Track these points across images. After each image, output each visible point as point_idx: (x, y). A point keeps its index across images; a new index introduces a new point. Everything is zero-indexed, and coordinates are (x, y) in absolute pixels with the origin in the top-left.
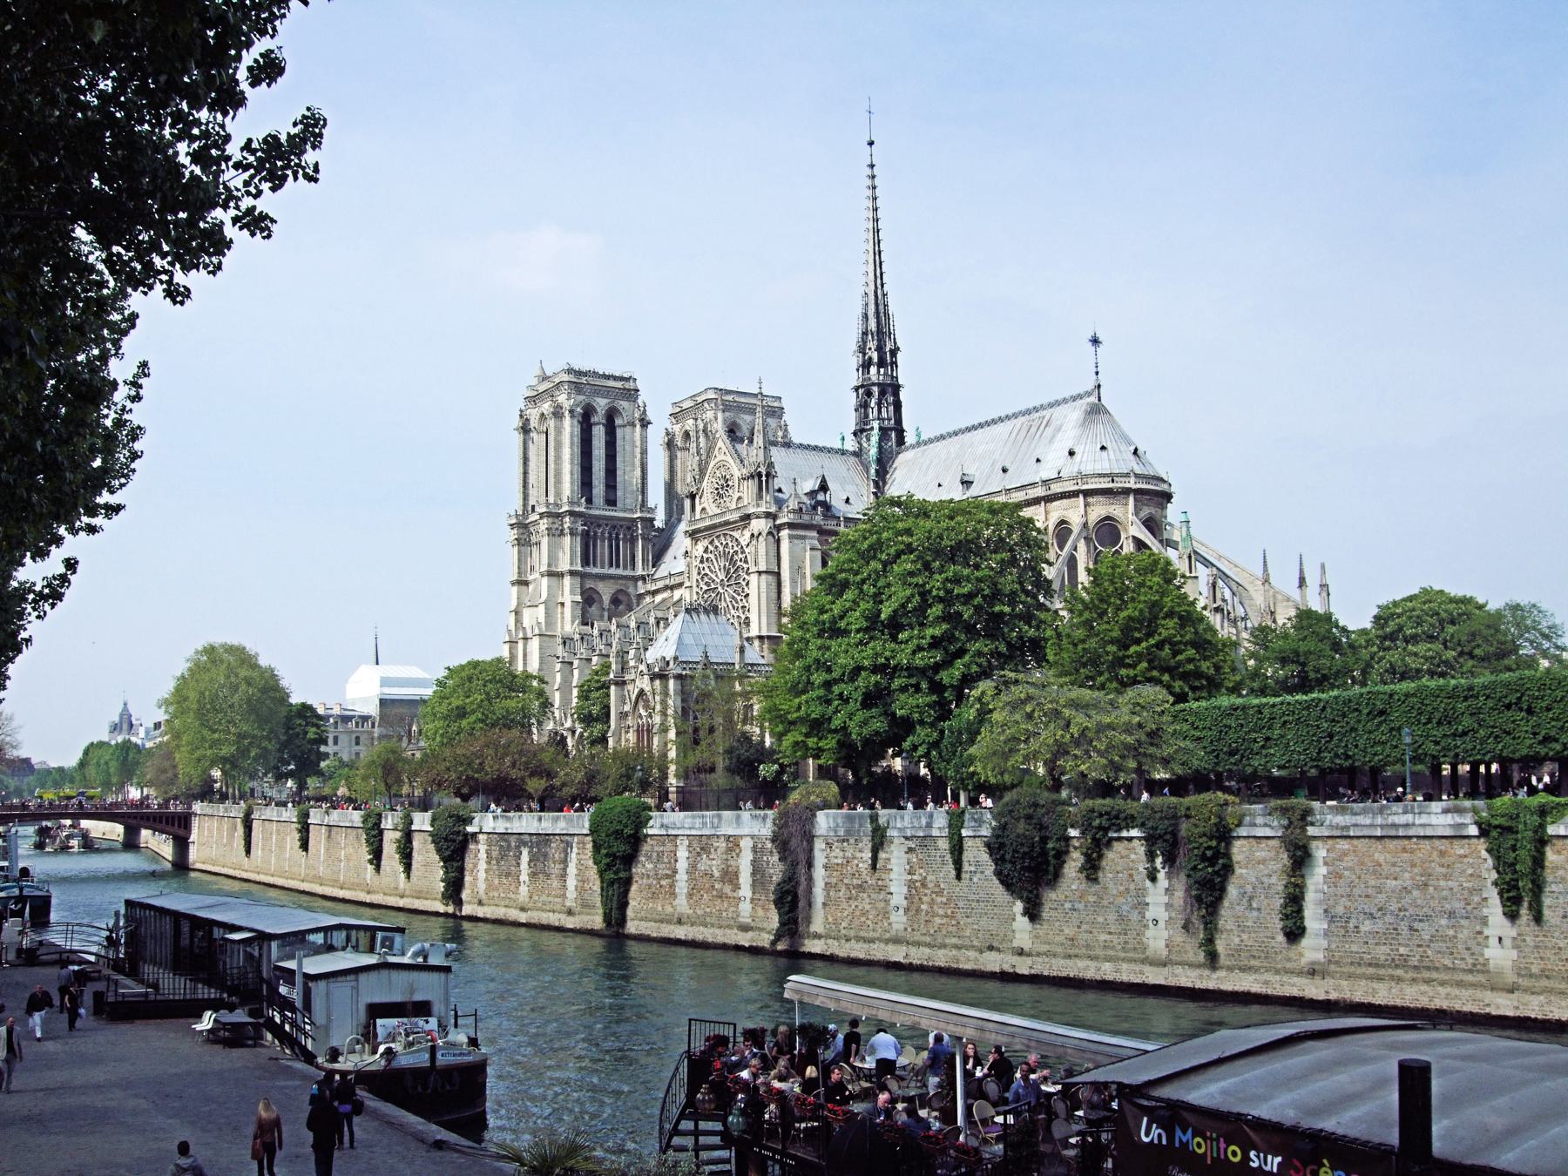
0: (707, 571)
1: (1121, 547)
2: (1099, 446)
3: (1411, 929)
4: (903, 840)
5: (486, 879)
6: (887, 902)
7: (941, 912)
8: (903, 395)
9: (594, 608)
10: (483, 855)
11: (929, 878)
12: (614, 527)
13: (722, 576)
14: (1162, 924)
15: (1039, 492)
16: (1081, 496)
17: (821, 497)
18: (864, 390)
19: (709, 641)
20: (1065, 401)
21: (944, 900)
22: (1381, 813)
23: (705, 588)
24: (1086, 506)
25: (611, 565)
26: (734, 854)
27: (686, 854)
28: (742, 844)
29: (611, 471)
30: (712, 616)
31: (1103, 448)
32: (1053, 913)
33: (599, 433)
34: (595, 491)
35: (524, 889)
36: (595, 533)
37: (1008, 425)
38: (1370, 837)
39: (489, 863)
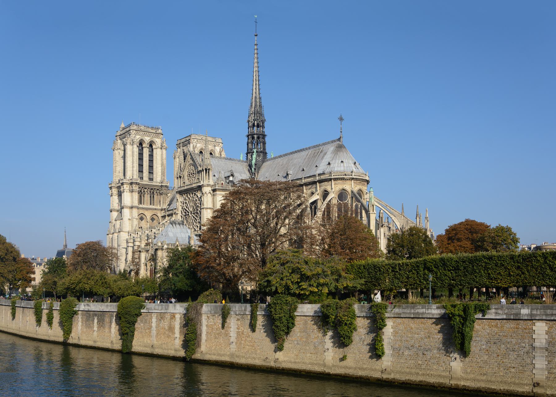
0: (185, 208)
1: (348, 201)
2: (340, 161)
3: (423, 354)
4: (235, 315)
6: (229, 340)
7: (249, 344)
8: (267, 139)
9: (143, 221)
12: (152, 189)
13: (191, 209)
15: (317, 178)
16: (333, 180)
18: (251, 136)
19: (179, 235)
20: (328, 143)
21: (250, 339)
22: (414, 308)
23: (184, 214)
24: (335, 184)
25: (151, 204)
26: (173, 320)
27: (156, 320)
28: (176, 316)
29: (151, 167)
30: (181, 226)
31: (342, 162)
32: (290, 345)
34: (144, 175)
36: (144, 191)
37: (307, 152)
38: (409, 318)
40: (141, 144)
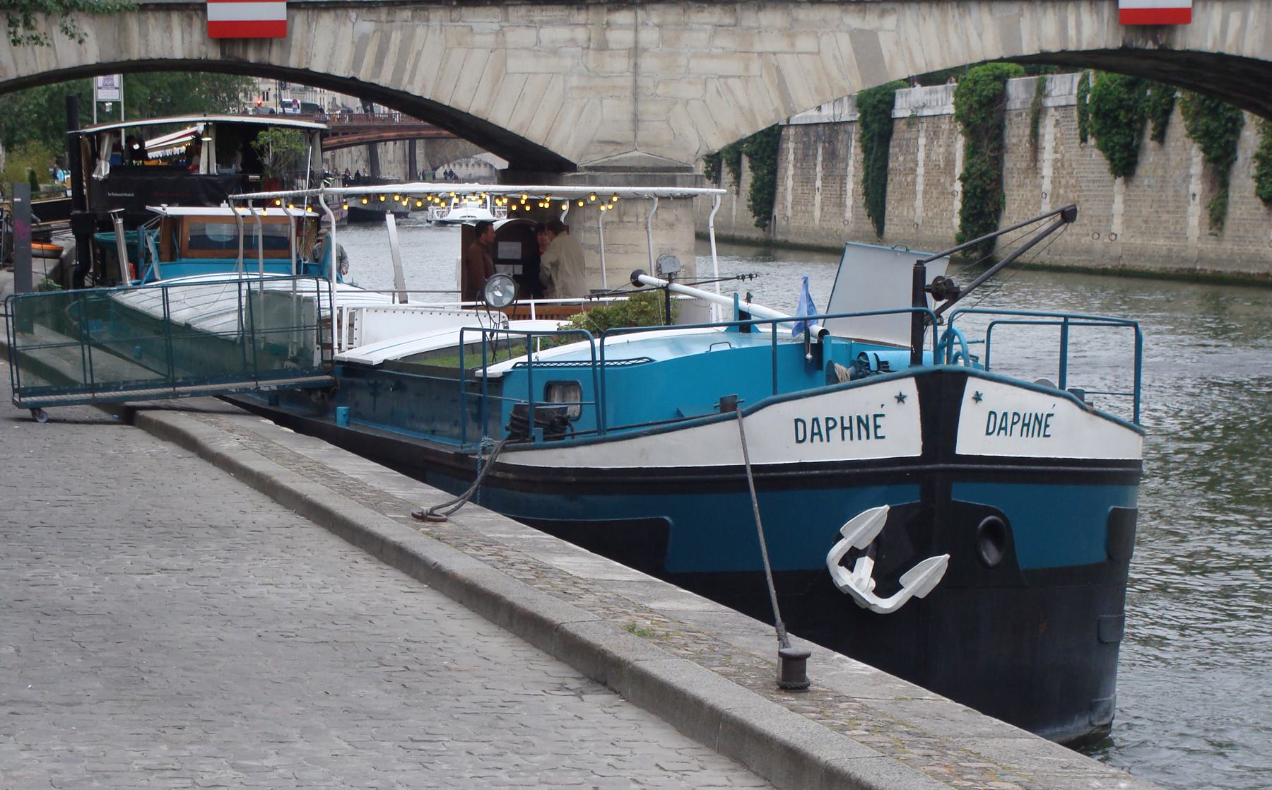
4: (1053, 110)
5: (793, 189)
10: (791, 157)
11: (1067, 155)
14: (1198, 198)
35: (818, 198)
39: (795, 166)
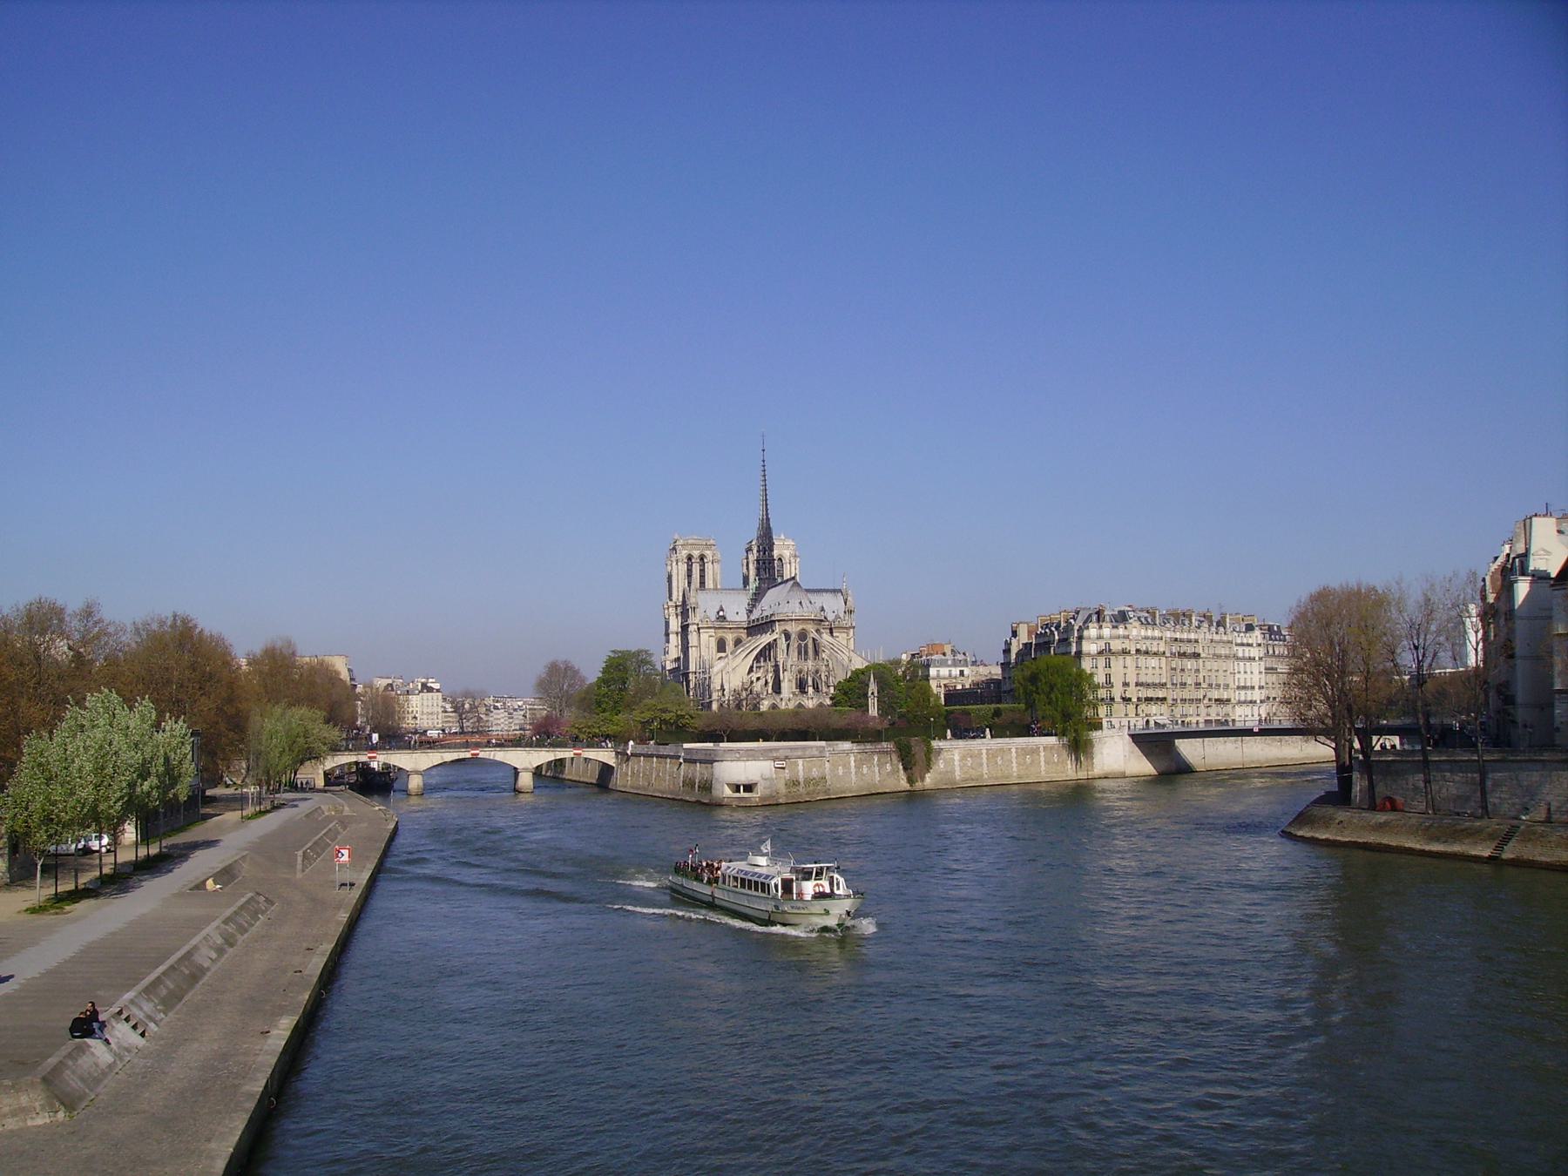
17: (721, 613)
33: (696, 569)
40: (690, 558)
